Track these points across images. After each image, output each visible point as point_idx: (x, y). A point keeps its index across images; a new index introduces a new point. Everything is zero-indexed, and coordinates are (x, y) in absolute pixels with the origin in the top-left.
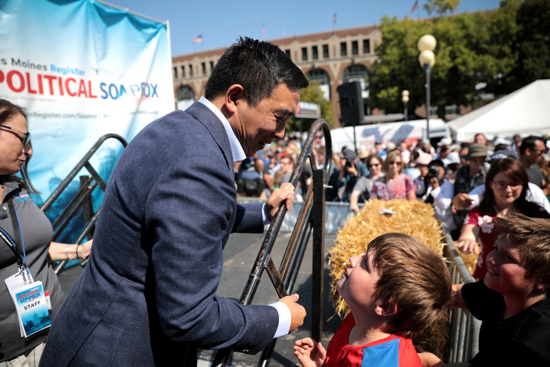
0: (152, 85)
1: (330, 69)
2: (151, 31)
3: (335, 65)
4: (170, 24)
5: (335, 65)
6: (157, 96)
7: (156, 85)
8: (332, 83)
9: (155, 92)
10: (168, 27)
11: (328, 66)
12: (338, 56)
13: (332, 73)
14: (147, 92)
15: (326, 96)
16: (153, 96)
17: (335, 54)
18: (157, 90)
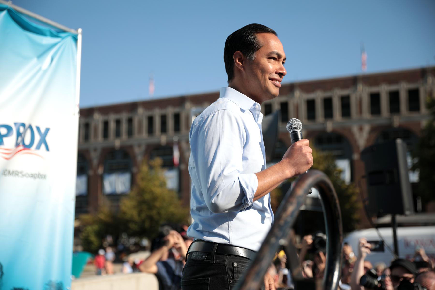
0: (38, 128)
1: (352, 135)
2: (47, 41)
3: (361, 129)
4: (83, 34)
5: (361, 129)
6: (47, 149)
7: (47, 130)
8: (356, 156)
9: (43, 141)
10: (80, 38)
11: (350, 130)
12: (367, 115)
13: (356, 141)
14: (27, 141)
15: (347, 176)
16: (38, 147)
17: (360, 111)
18: (48, 139)
